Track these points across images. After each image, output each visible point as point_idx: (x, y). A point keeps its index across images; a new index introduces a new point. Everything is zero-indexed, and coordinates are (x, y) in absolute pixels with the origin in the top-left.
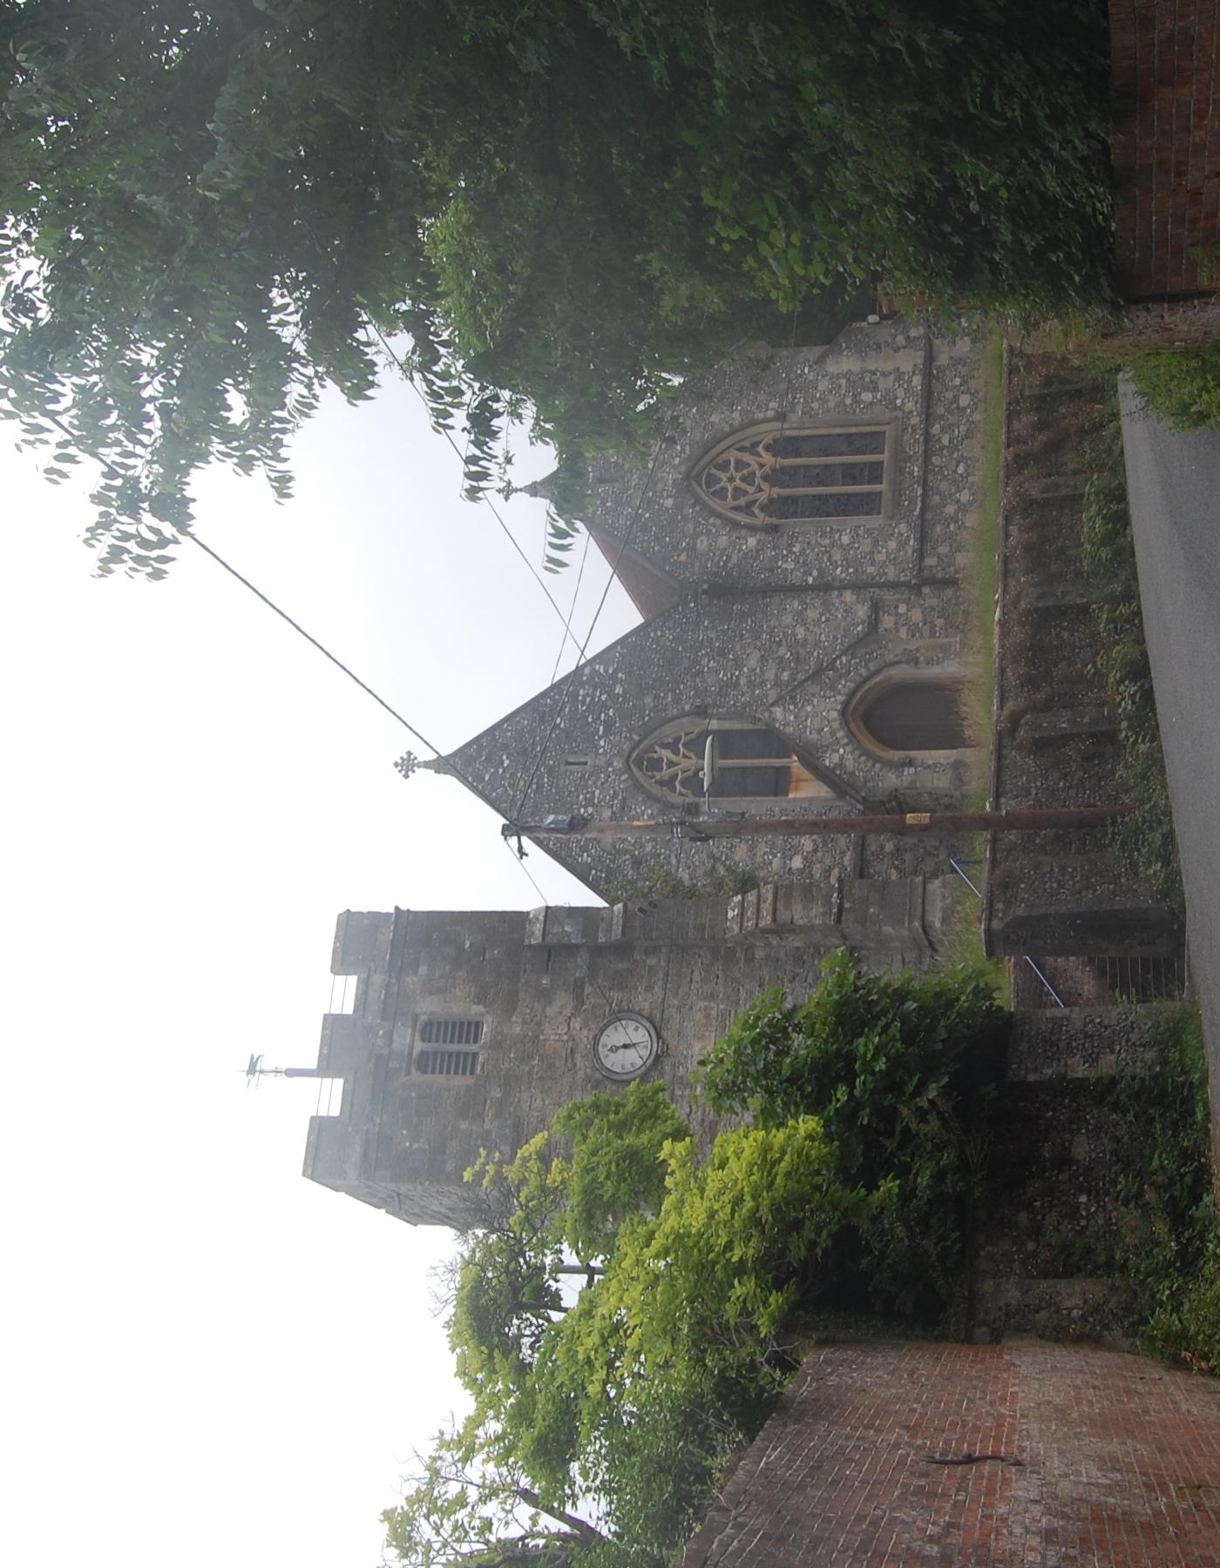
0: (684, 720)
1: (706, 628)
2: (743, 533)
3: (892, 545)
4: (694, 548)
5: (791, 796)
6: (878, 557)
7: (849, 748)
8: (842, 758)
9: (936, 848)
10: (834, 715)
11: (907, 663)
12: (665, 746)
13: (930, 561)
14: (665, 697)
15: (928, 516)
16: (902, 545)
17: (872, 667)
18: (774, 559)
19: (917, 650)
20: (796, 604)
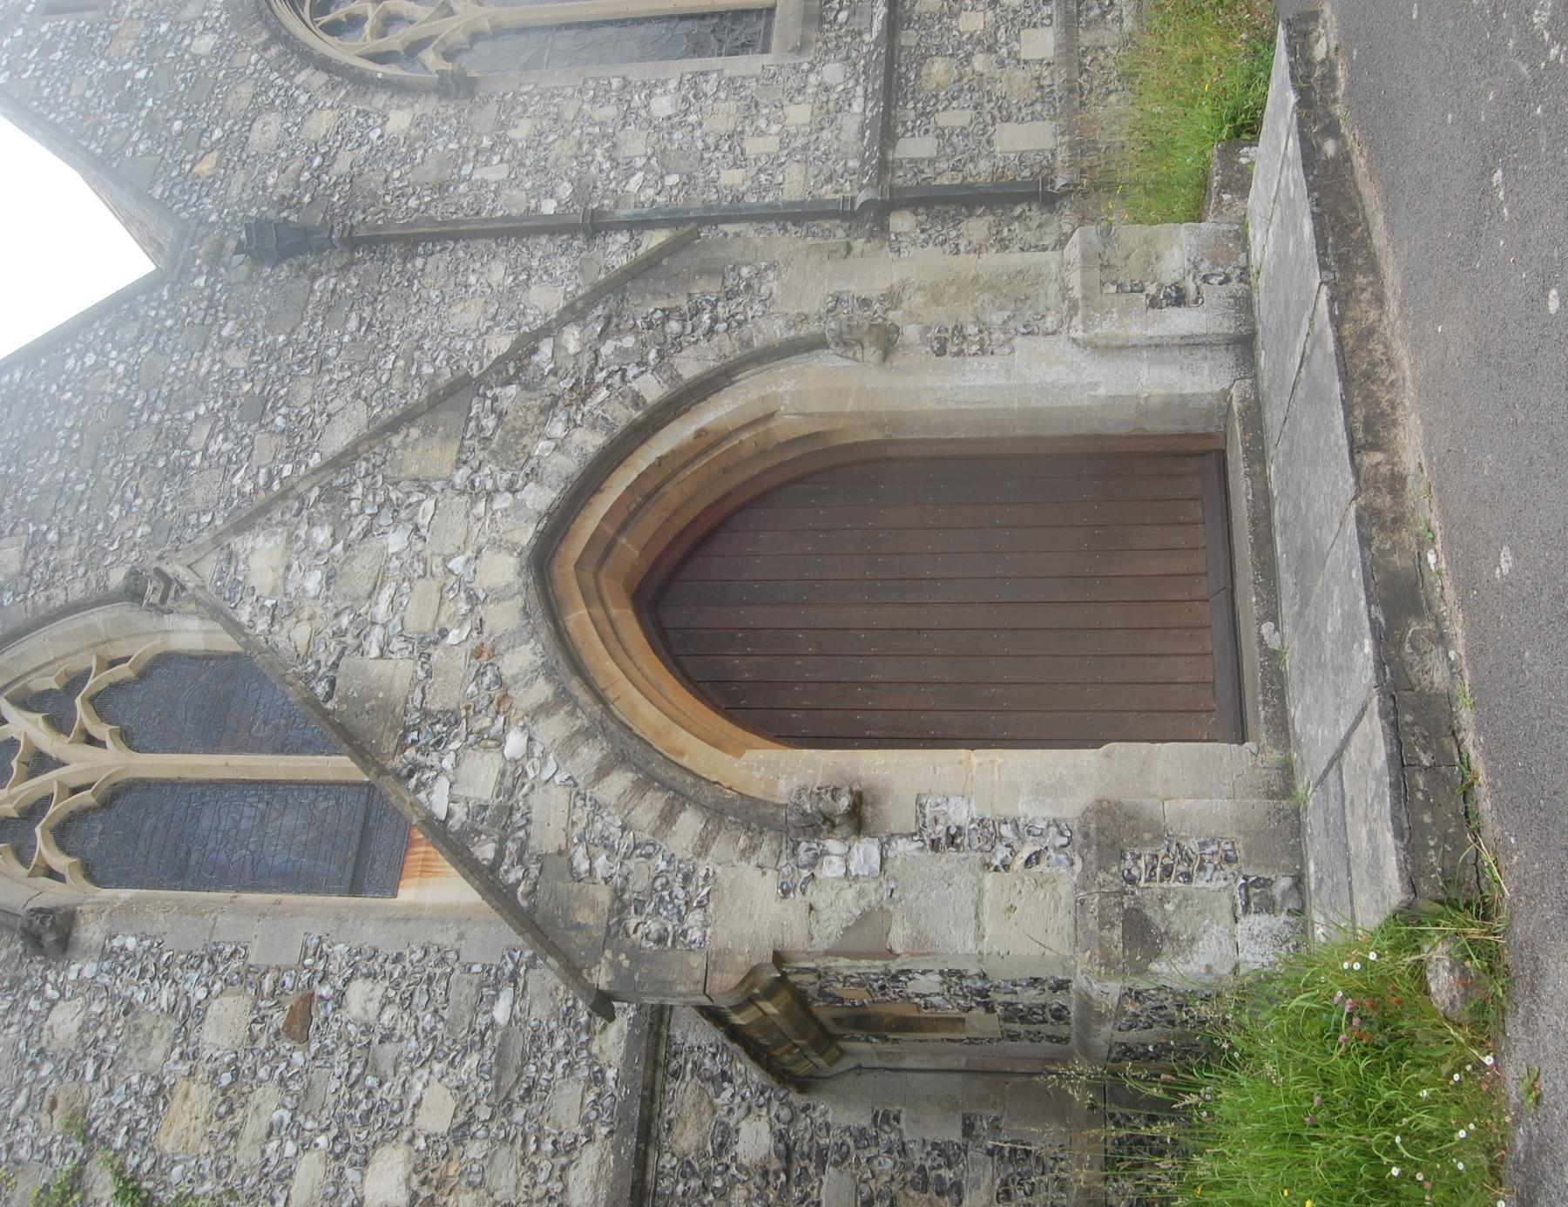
0: (98, 617)
1: (226, 344)
2: (380, 100)
3: (799, 114)
4: (244, 143)
5: (408, 893)
6: (753, 146)
7: (553, 729)
8: (513, 779)
9: (948, 1154)
10: (503, 570)
11: (847, 341)
12: (28, 702)
13: (914, 147)
14: (59, 545)
15: (908, 38)
16: (828, 114)
17: (690, 366)
18: (458, 159)
19: (892, 299)
20: (498, 273)
